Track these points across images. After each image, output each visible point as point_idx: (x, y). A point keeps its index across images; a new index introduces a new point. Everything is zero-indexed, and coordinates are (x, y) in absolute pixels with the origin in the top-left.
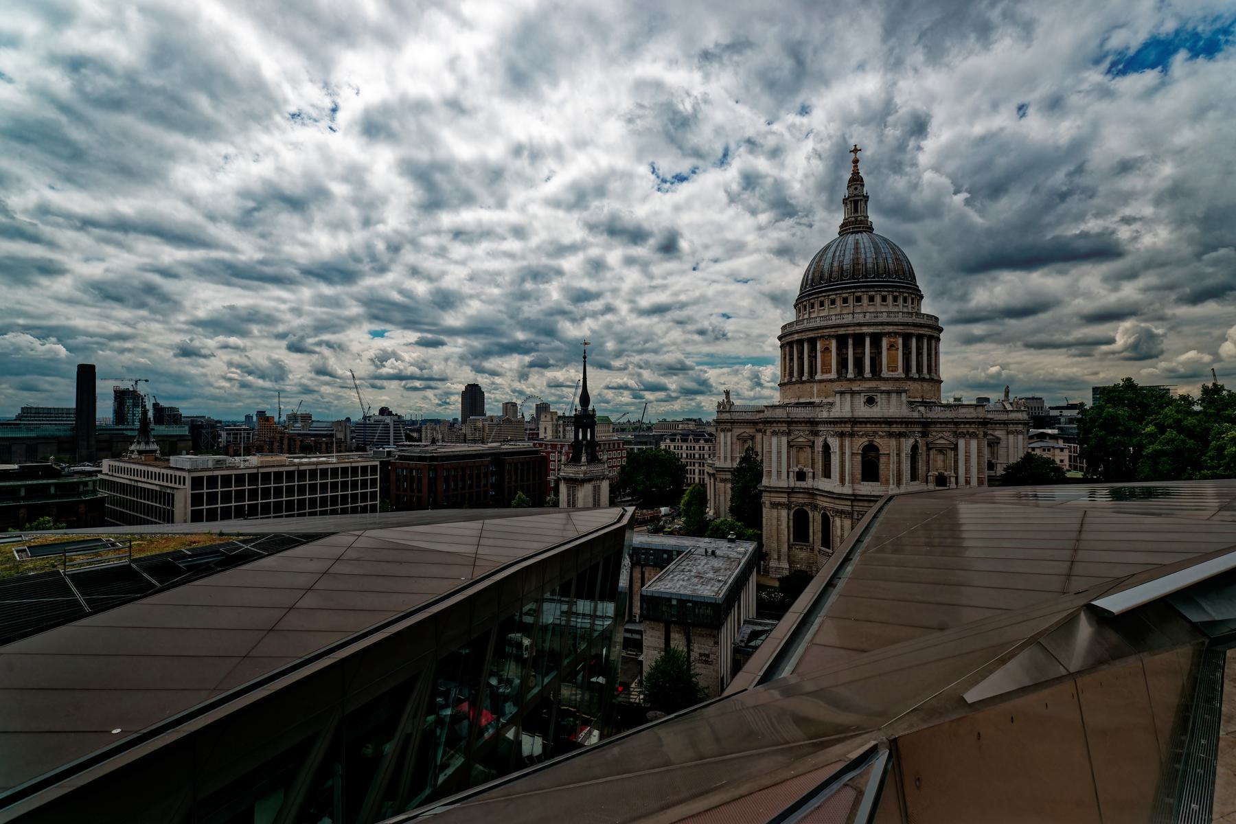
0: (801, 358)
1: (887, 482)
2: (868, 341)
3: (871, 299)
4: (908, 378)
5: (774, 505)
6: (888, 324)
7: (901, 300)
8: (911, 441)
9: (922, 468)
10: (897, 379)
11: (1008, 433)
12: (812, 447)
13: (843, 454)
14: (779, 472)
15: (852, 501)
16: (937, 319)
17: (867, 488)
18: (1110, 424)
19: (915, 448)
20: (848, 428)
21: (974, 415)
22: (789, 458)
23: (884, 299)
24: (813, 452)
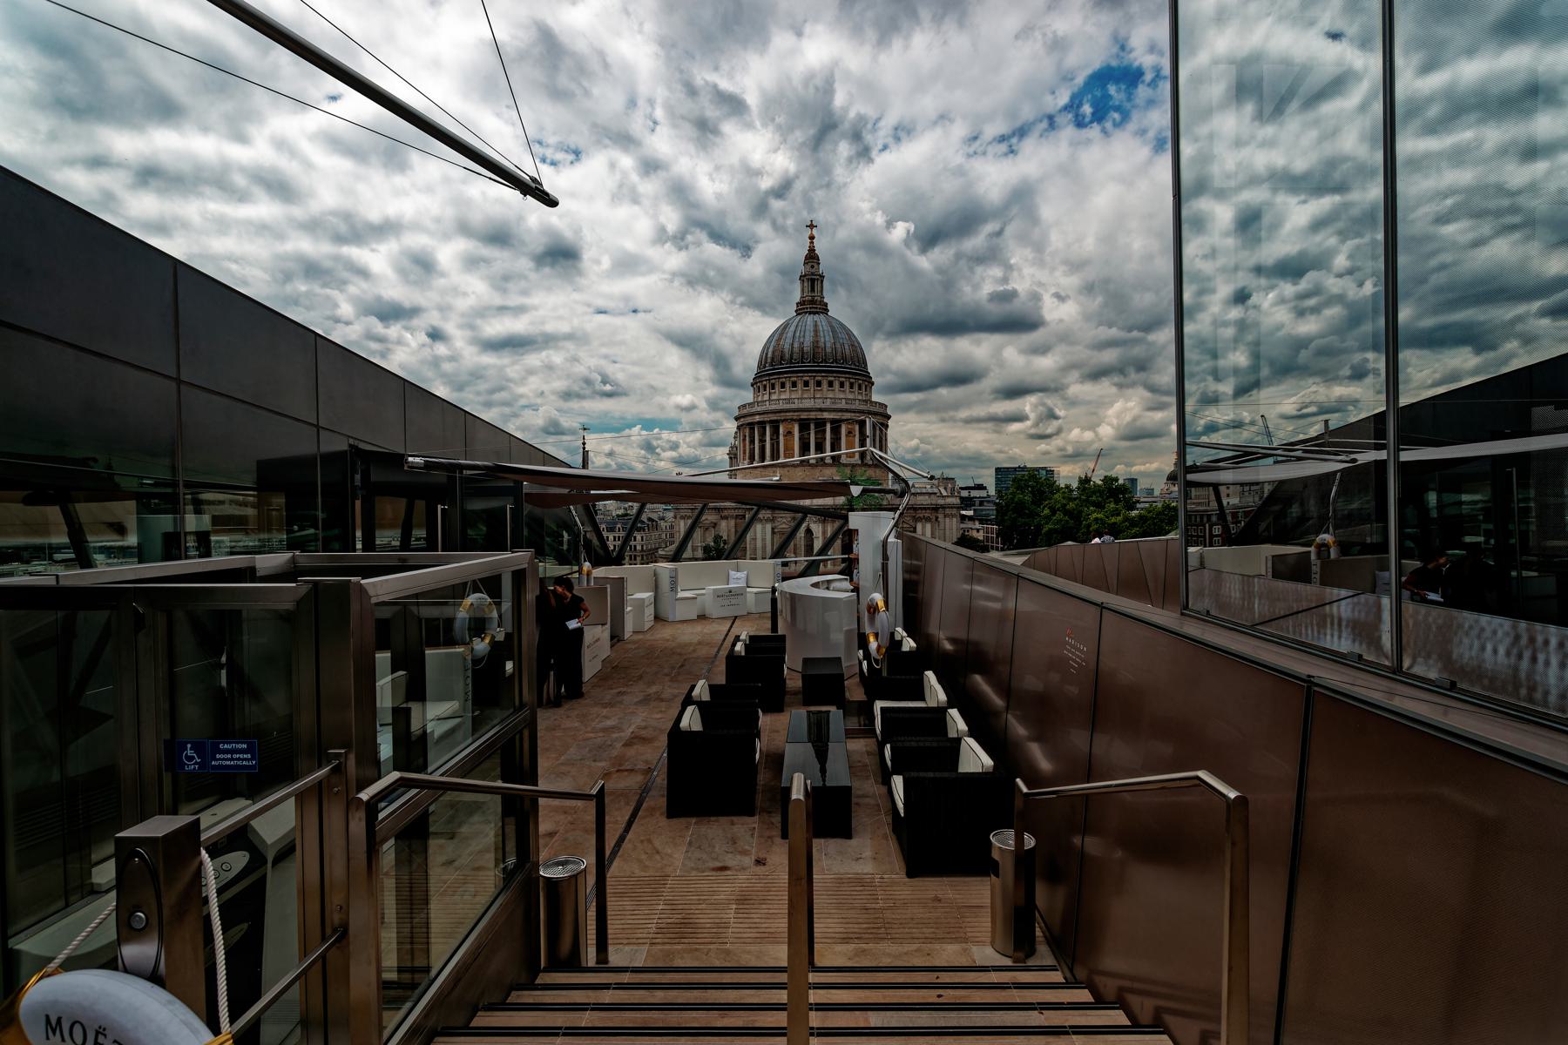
0: (762, 441)
3: (831, 384)
6: (847, 411)
18: (1020, 508)
23: (842, 385)
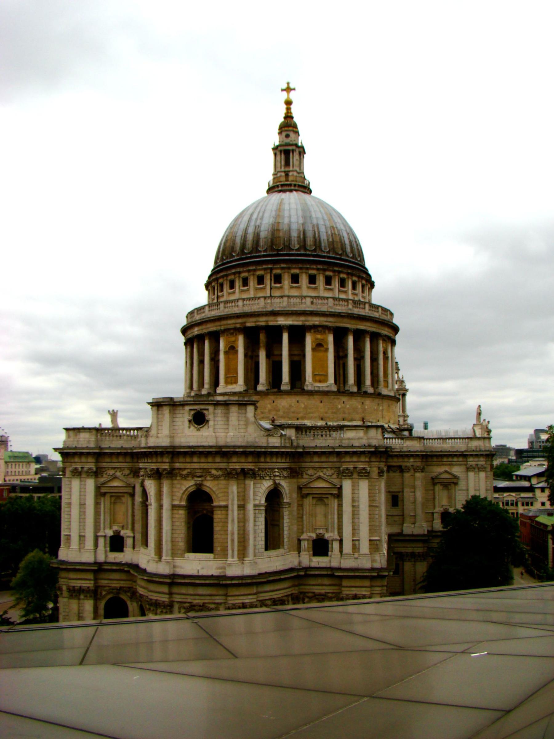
1: (224, 554)
2: (285, 337)
4: (341, 391)
5: (75, 593)
7: (336, 283)
8: (266, 485)
10: (326, 393)
11: (468, 469)
14: (82, 537)
15: (171, 585)
16: (392, 314)
17: (196, 564)
21: (364, 442)
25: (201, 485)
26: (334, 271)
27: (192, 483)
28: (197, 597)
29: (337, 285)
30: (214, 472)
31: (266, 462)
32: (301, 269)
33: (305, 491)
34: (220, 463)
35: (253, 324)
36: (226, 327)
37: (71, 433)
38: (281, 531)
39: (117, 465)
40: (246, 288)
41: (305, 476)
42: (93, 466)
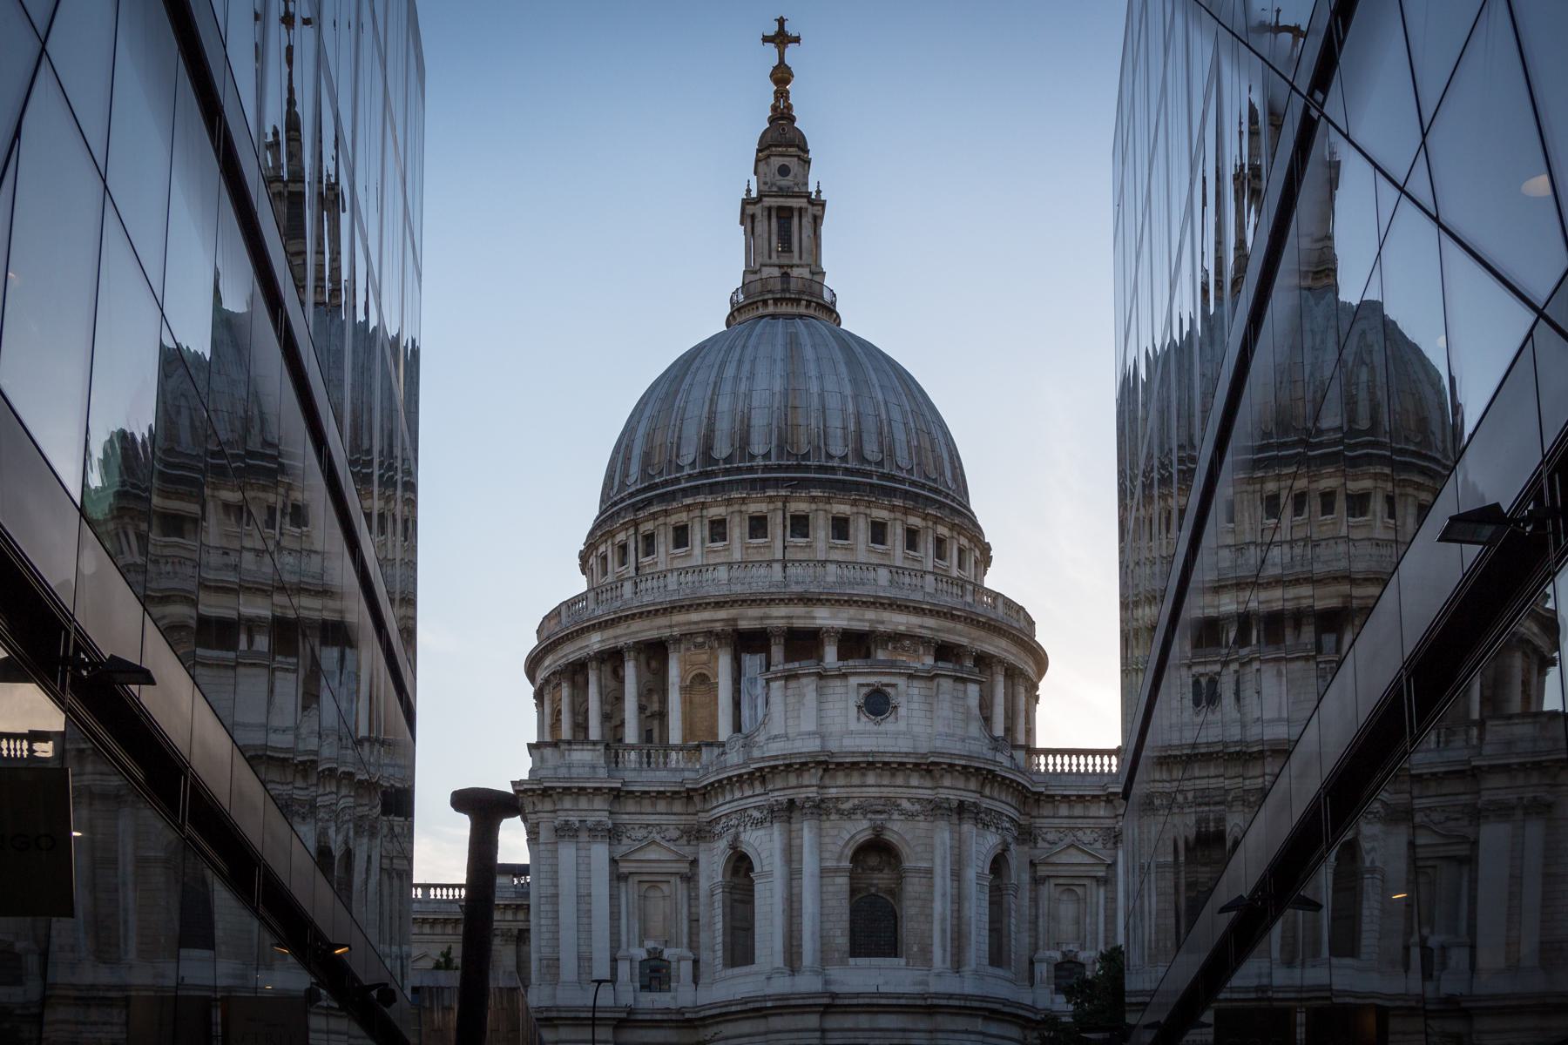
3: (840, 527)
7: (927, 547)
8: (992, 840)
9: (1019, 942)
12: (690, 879)
13: (793, 874)
14: (584, 960)
19: (998, 864)
20: (807, 788)
22: (614, 916)
24: (693, 899)
25: (883, 828)
26: (925, 517)
27: (865, 824)
28: (877, 1034)
29: (931, 552)
30: (905, 804)
31: (992, 798)
32: (854, 503)
33: (1042, 871)
34: (919, 787)
35: (755, 625)
36: (685, 629)
37: (548, 752)
38: (1005, 940)
39: (652, 819)
40: (719, 545)
41: (1041, 844)
42: (603, 817)
